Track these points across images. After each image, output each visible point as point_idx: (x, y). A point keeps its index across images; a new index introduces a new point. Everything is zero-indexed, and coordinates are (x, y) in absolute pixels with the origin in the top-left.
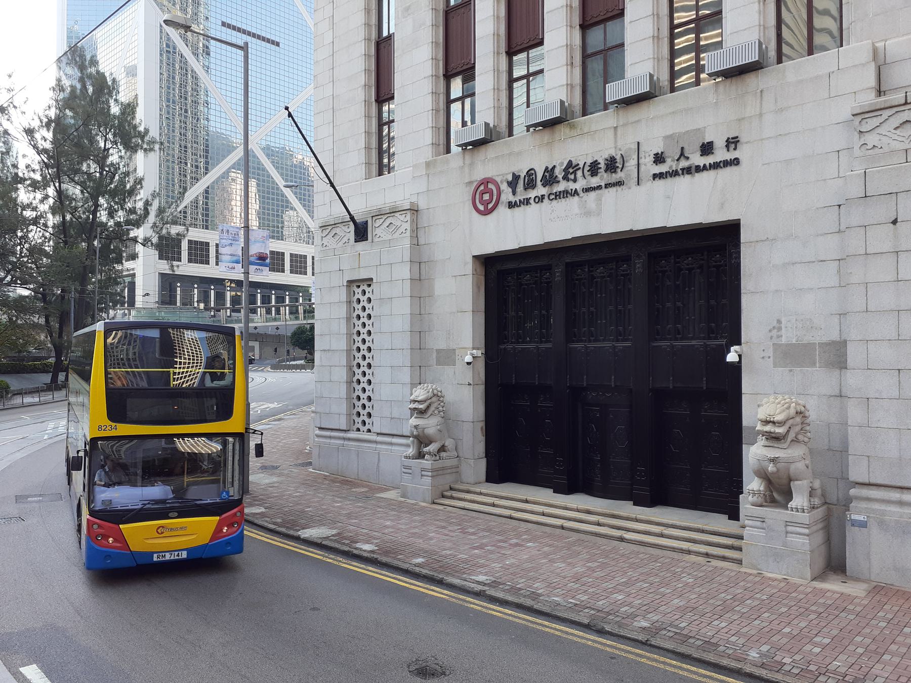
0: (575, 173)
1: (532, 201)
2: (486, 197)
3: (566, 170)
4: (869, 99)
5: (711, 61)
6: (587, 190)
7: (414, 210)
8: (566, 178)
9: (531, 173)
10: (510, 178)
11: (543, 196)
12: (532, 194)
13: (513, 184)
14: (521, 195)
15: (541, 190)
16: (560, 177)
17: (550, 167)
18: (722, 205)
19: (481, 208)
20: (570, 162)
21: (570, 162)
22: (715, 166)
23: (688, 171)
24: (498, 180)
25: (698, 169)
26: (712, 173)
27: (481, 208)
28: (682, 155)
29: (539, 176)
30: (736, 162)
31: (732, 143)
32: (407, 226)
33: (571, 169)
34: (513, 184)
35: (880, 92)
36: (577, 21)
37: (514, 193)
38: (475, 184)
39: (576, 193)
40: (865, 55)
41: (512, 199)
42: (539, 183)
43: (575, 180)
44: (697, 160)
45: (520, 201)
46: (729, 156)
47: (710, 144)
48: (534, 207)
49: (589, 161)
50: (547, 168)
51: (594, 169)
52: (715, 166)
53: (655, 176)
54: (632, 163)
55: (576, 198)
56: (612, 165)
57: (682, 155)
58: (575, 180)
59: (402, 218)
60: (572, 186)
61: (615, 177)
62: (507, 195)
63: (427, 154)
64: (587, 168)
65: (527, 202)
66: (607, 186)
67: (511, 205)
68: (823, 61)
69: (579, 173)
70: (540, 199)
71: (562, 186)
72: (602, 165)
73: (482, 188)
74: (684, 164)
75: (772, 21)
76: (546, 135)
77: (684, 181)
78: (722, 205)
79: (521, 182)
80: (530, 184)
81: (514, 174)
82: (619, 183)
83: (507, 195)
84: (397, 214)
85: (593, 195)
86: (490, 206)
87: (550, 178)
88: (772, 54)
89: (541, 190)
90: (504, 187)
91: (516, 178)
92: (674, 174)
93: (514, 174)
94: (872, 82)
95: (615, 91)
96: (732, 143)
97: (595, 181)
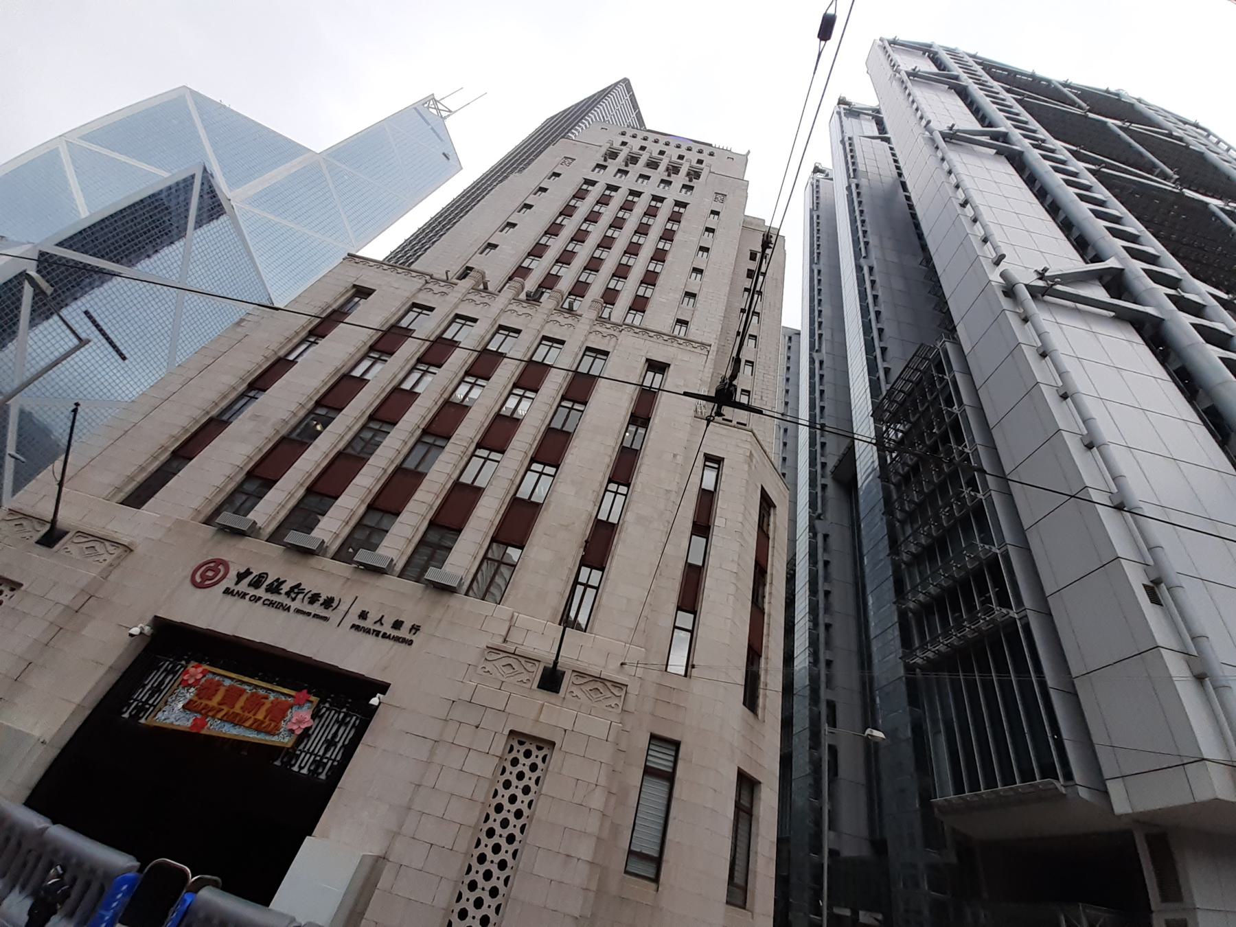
0: (298, 594)
3: (292, 589)
4: (497, 642)
5: (432, 574)
6: (298, 611)
7: (129, 549)
8: (288, 594)
9: (262, 577)
10: (242, 571)
12: (252, 591)
15: (261, 592)
16: (283, 592)
18: (385, 668)
19: (198, 580)
20: (300, 584)
21: (300, 584)
22: (397, 639)
23: (377, 633)
25: (385, 636)
26: (392, 642)
27: (198, 580)
28: (380, 621)
30: (410, 643)
31: (415, 629)
32: (109, 559)
34: (241, 577)
35: (505, 641)
36: (368, 501)
40: (507, 617)
41: (232, 586)
42: (264, 586)
44: (387, 628)
46: (408, 637)
47: (402, 622)
49: (314, 592)
51: (314, 599)
52: (397, 639)
53: (353, 626)
54: (343, 607)
56: (328, 603)
57: (380, 621)
58: (294, 599)
59: (111, 549)
60: (287, 602)
61: (323, 613)
63: (186, 515)
65: (243, 595)
66: (316, 616)
67: (227, 591)
68: (488, 606)
69: (301, 596)
70: (256, 599)
72: (322, 600)
74: (377, 627)
75: (473, 570)
76: (296, 557)
77: (371, 639)
78: (385, 668)
80: (256, 584)
82: (326, 619)
84: (107, 544)
85: (300, 617)
87: (275, 588)
88: (465, 587)
90: (233, 574)
91: (248, 572)
92: (368, 631)
94: (504, 633)
95: (363, 556)
96: (415, 629)
97: (309, 608)
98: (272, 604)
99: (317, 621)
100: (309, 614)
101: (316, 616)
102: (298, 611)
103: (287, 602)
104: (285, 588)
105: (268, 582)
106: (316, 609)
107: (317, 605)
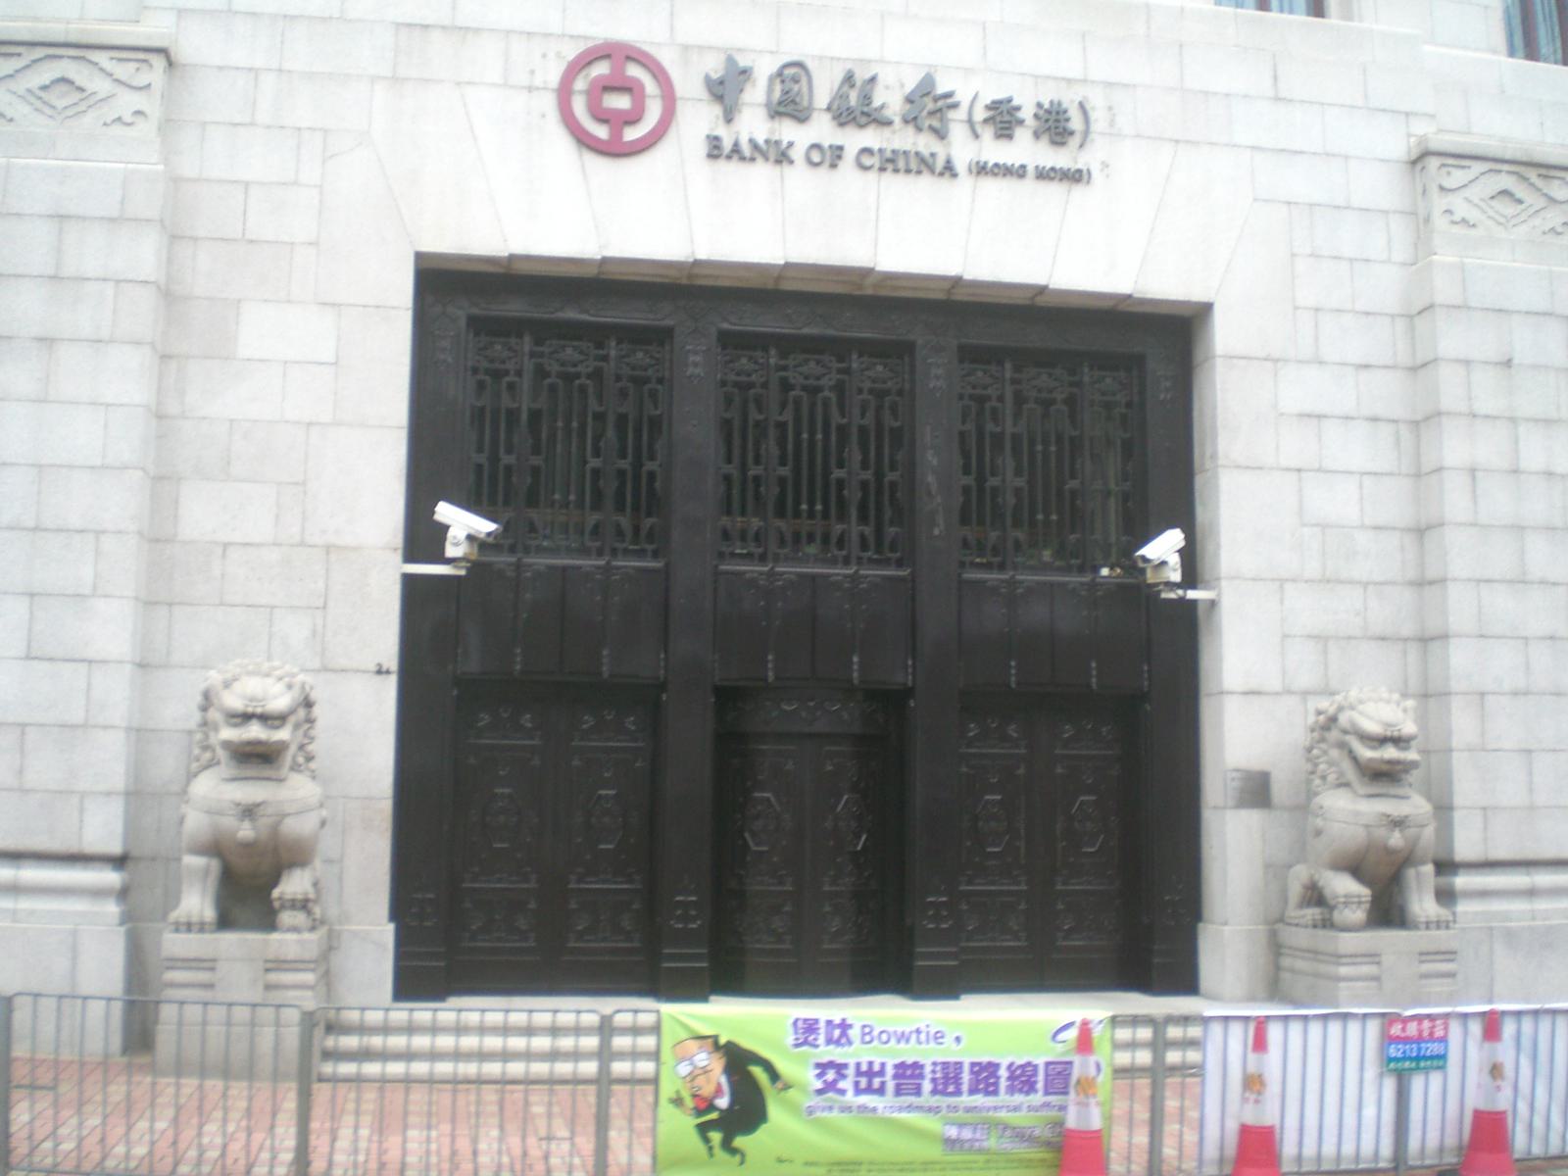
1: (798, 154)
2: (621, 102)
6: (981, 170)
11: (837, 152)
13: (725, 90)
14: (753, 124)
15: (821, 129)
17: (861, 75)
19: (601, 132)
24: (667, 58)
27: (601, 132)
29: (823, 92)
33: (929, 107)
34: (725, 90)
37: (729, 118)
38: (571, 52)
39: (949, 170)
43: (941, 134)
45: (755, 146)
48: (798, 177)
49: (987, 98)
50: (849, 79)
51: (1003, 119)
55: (945, 183)
56: (1055, 126)
58: (941, 134)
60: (925, 143)
61: (1060, 158)
62: (697, 119)
64: (980, 114)
65: (781, 156)
66: (1044, 175)
67: (715, 149)
71: (903, 139)
73: (601, 69)
79: (756, 94)
80: (789, 106)
81: (730, 61)
82: (1074, 177)
83: (697, 119)
85: (991, 186)
86: (632, 134)
89: (821, 129)
93: (730, 61)
98: (891, 162)
99: (1055, 190)
100: (1020, 172)
101: (1044, 175)
102: (981, 170)
103: (925, 143)
104: (890, 98)
105: (822, 96)
106: (1024, 149)
107: (1023, 136)
